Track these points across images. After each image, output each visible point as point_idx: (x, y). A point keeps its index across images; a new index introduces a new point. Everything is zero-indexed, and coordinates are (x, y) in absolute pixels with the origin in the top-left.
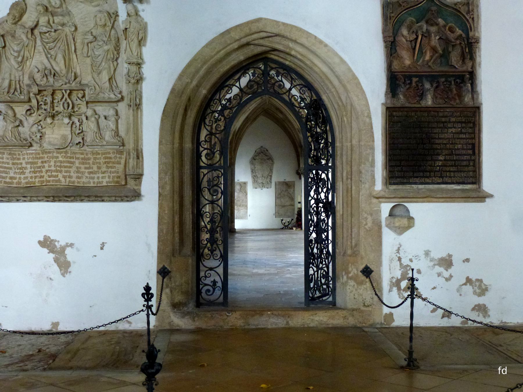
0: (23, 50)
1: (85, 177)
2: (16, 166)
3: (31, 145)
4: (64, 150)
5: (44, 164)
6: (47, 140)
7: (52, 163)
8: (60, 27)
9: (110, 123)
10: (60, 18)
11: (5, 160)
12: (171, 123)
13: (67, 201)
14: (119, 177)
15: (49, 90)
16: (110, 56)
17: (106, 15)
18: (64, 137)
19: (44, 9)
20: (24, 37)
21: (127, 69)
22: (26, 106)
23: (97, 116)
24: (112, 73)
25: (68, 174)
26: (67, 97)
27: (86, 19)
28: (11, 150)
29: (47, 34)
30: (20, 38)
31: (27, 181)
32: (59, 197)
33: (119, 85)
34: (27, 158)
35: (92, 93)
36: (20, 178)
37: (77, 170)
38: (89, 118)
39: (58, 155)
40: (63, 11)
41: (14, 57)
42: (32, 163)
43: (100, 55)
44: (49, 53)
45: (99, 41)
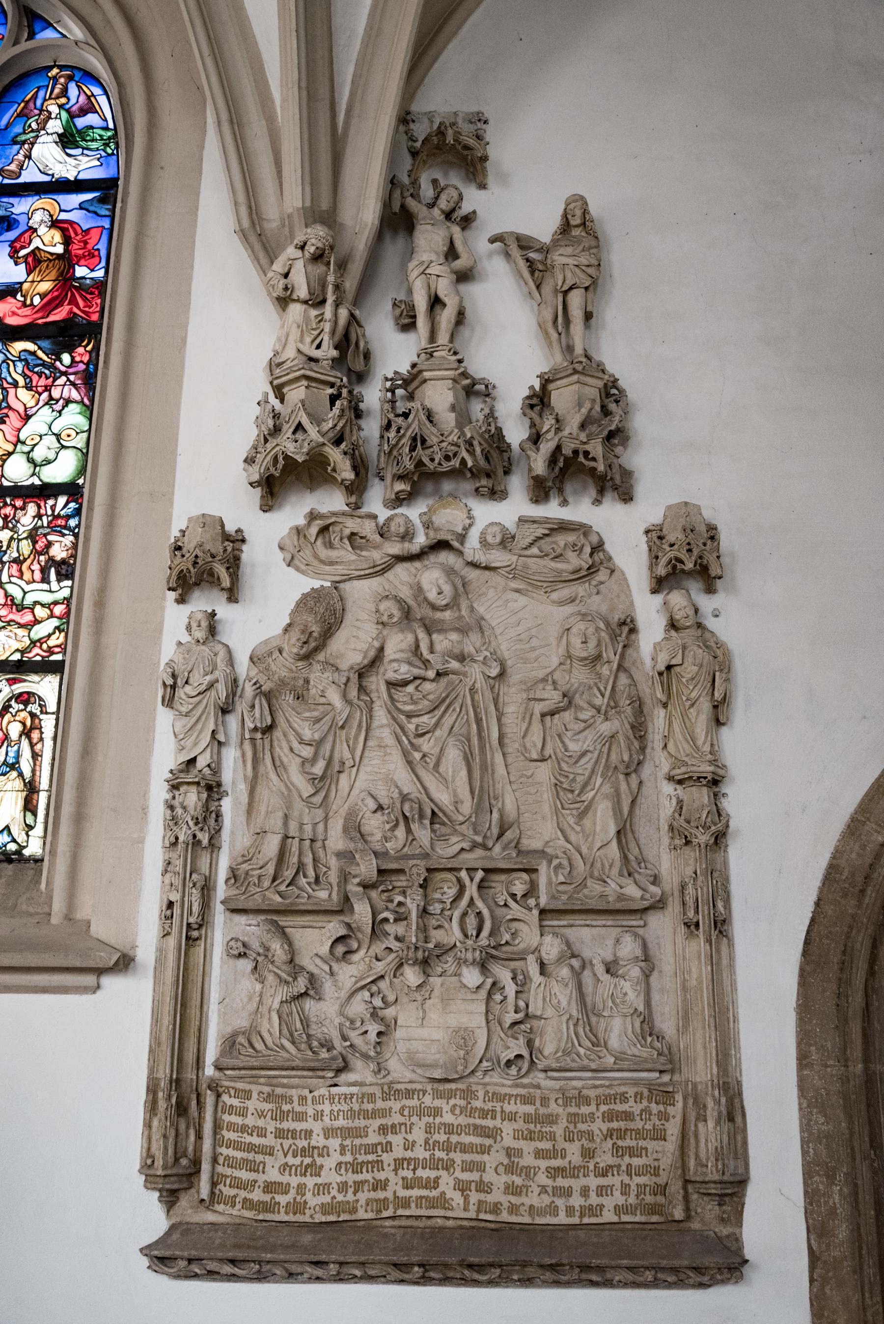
0: (330, 738)
1: (537, 1190)
2: (291, 1141)
3: (344, 1068)
4: (461, 1086)
5: (390, 1137)
6: (401, 1047)
7: (418, 1135)
8: (455, 665)
9: (627, 986)
10: (454, 636)
11: (250, 1121)
12: (835, 987)
13: (476, 1283)
14: (662, 1190)
15: (414, 870)
16: (620, 754)
17: (602, 625)
18: (463, 1038)
19: (401, 608)
20: (334, 697)
21: (674, 801)
22: (334, 928)
23: (575, 963)
24: (626, 811)
25: (475, 1176)
26: (476, 895)
27: (534, 642)
28: (275, 1081)
29: (410, 688)
30: (323, 700)
31: (327, 1199)
32: (446, 1265)
33: (650, 855)
34: (332, 1111)
35: (561, 878)
36: (301, 1188)
37: (506, 1161)
38: (550, 969)
39: (438, 1103)
40: (460, 617)
41: (298, 760)
42: (347, 1133)
43: (584, 754)
44: (416, 748)
45: (582, 709)
